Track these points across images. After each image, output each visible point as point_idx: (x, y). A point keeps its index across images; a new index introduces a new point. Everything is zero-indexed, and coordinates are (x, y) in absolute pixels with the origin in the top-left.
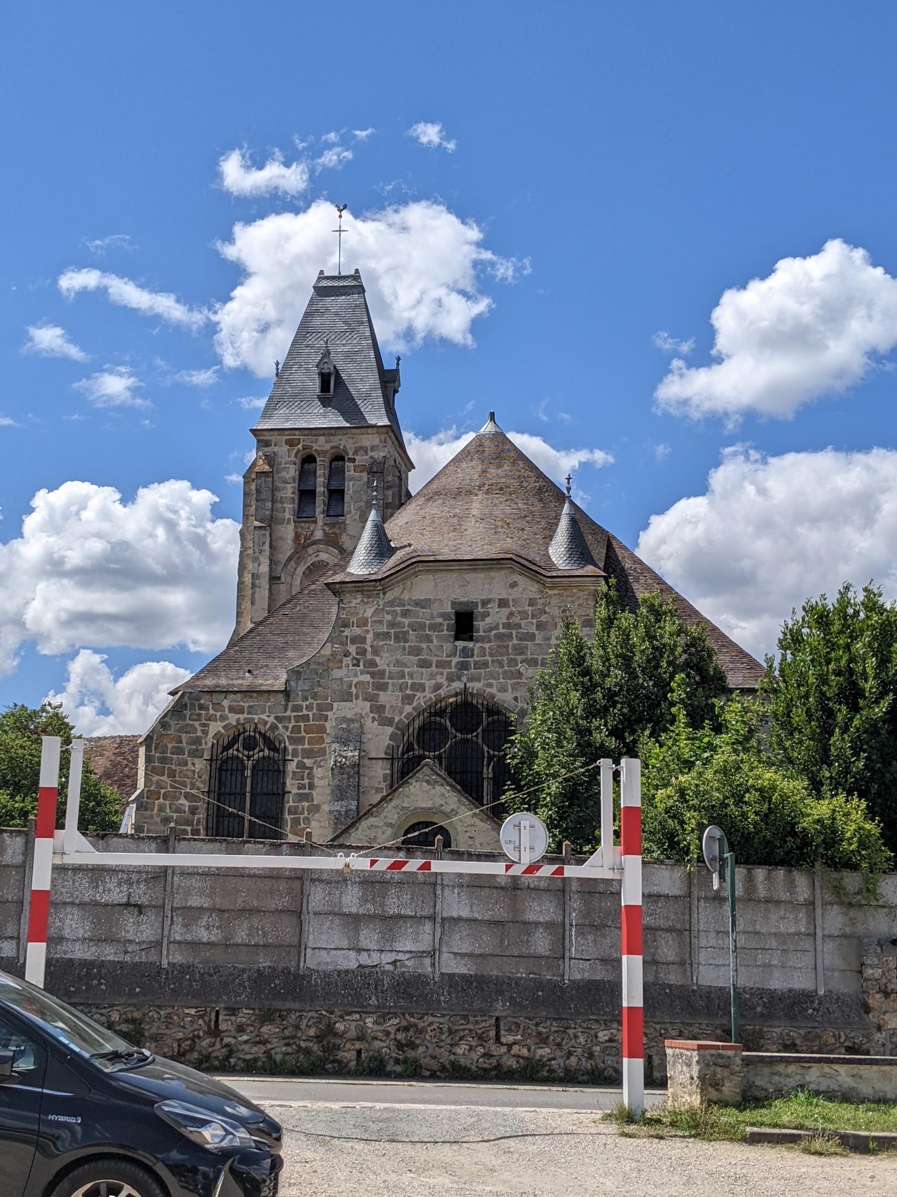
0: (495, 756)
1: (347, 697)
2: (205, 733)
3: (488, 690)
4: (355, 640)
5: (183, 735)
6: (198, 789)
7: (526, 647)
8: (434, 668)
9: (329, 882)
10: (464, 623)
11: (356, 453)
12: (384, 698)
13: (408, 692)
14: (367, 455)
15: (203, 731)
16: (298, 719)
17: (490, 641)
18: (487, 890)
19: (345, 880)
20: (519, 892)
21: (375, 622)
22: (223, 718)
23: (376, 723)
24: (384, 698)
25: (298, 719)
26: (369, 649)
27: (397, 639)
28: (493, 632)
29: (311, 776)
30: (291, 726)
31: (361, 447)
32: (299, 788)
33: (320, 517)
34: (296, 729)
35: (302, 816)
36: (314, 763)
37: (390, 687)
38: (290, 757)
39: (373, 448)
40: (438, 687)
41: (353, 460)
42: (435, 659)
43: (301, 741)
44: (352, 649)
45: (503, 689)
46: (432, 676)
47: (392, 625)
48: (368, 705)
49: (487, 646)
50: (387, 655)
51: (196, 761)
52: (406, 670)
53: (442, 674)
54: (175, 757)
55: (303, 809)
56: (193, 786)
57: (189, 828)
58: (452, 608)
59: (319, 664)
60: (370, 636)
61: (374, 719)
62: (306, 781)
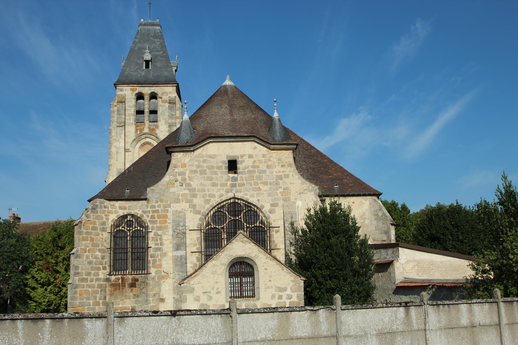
0: (249, 227)
1: (177, 201)
2: (107, 219)
3: (245, 197)
4: (180, 174)
5: (97, 221)
6: (105, 247)
7: (262, 176)
8: (219, 187)
9: (356, 337)
10: (232, 166)
11: (162, 94)
12: (196, 201)
13: (207, 198)
15: (107, 219)
16: (153, 212)
17: (245, 174)
18: (456, 330)
19: (366, 334)
20: (475, 328)
21: (190, 165)
22: (116, 212)
23: (192, 213)
24: (196, 201)
25: (153, 212)
26: (187, 178)
27: (201, 173)
28: (246, 170)
29: (161, 239)
30: (150, 215)
31: (165, 92)
32: (155, 245)
33: (147, 122)
34: (153, 217)
35: (157, 259)
36: (163, 233)
37: (198, 196)
38: (150, 230)
39: (170, 93)
40: (221, 196)
41: (161, 98)
42: (219, 183)
43: (155, 222)
44: (179, 178)
45: (252, 196)
46: (218, 190)
47: (198, 166)
48: (188, 204)
49: (244, 176)
50: (196, 181)
51: (103, 233)
52: (206, 188)
53: (223, 189)
54: (93, 231)
55: (158, 255)
56: (102, 245)
57: (101, 266)
58: (227, 158)
59: (163, 185)
60: (187, 172)
61: (191, 211)
62: (159, 242)
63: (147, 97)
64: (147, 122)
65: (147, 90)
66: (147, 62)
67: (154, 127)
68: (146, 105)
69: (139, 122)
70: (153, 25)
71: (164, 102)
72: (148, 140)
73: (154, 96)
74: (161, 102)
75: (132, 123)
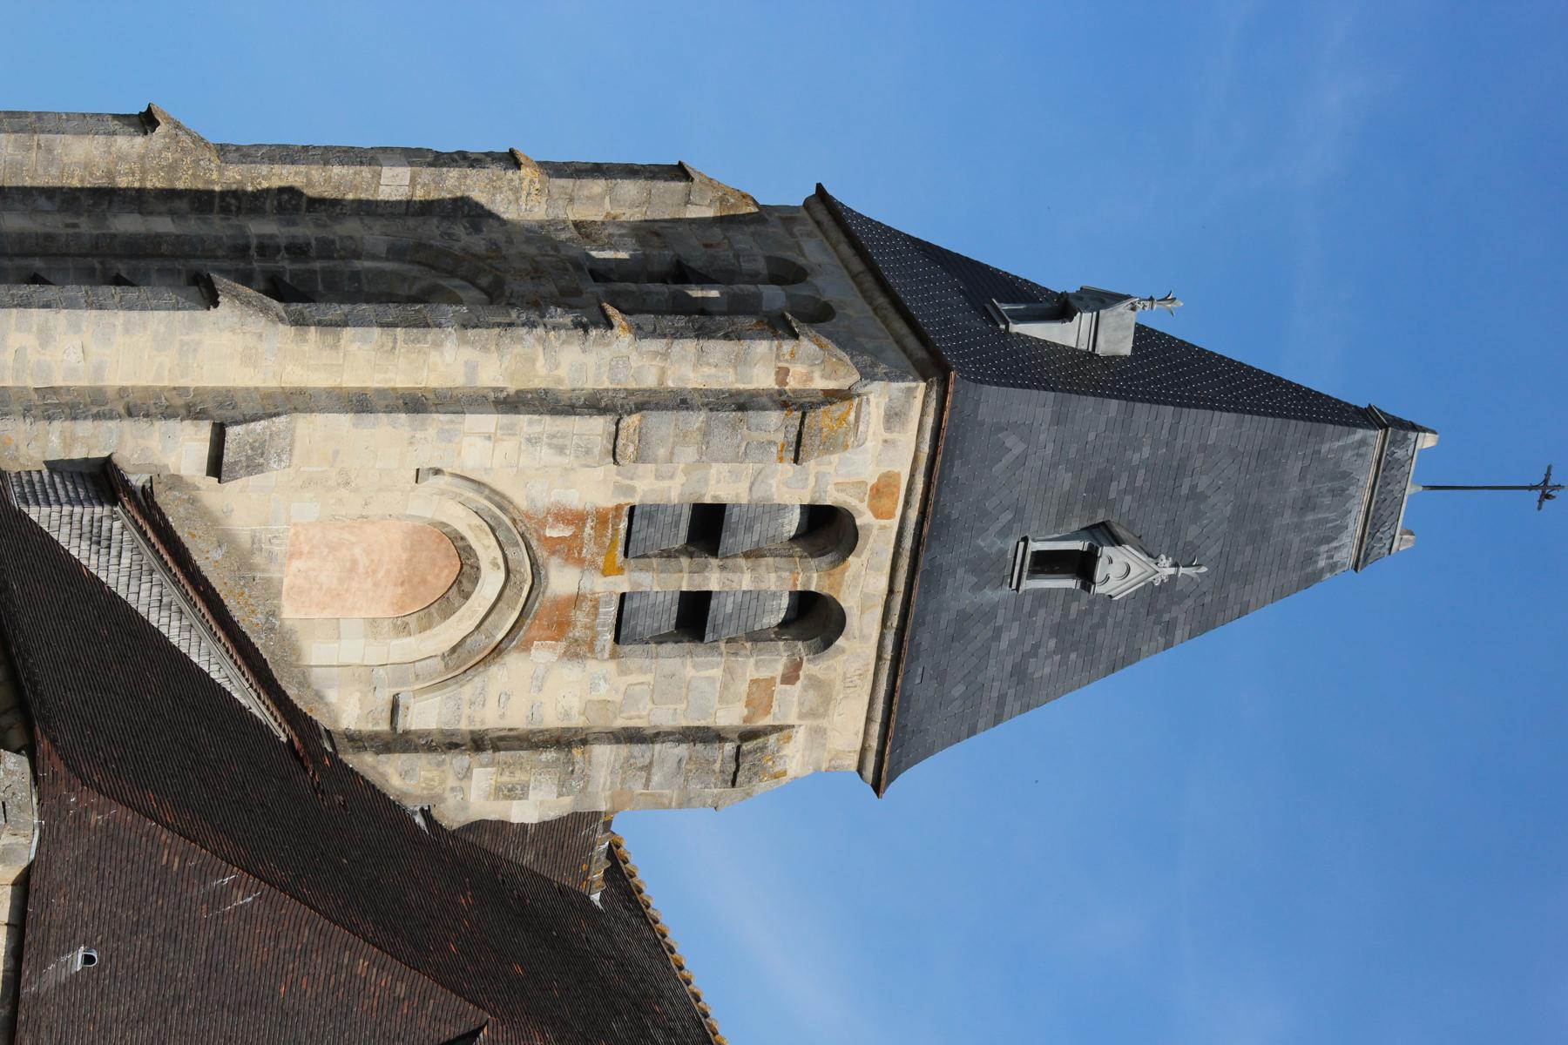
11: (816, 683)
14: (802, 716)
41: (790, 677)
63: (813, 578)
64: (622, 584)
65: (863, 584)
66: (1083, 566)
67: (577, 632)
68: (754, 583)
69: (633, 530)
70: (1375, 523)
71: (760, 696)
72: (491, 582)
73: (814, 619)
74: (764, 674)
75: (631, 490)
